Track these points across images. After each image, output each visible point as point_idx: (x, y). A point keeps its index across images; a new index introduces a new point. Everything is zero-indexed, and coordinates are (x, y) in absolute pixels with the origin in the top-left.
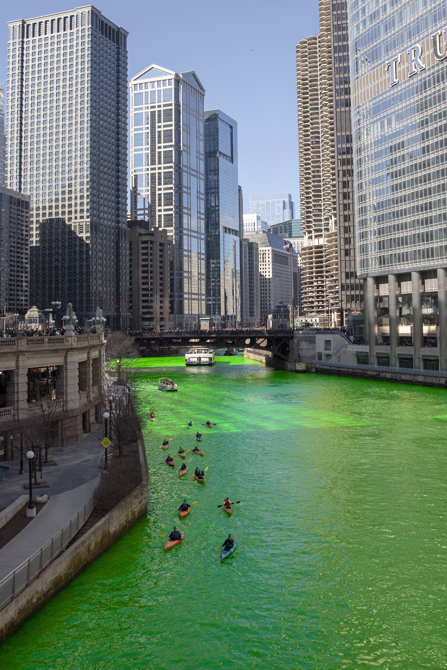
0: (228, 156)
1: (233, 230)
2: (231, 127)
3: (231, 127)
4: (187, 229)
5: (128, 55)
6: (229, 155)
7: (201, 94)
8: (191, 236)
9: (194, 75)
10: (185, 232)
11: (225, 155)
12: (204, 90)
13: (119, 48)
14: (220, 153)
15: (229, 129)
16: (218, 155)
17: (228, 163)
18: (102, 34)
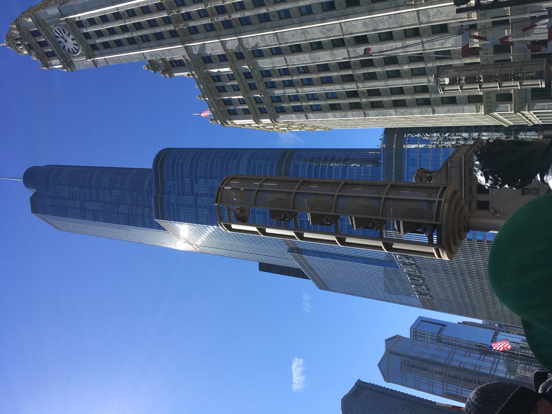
0: (442, 328)
1: (494, 335)
2: (422, 321)
3: (422, 321)
4: (491, 370)
5: (372, 383)
6: (440, 327)
7: (399, 338)
8: (496, 369)
9: (387, 341)
10: (492, 373)
11: (440, 330)
12: (398, 335)
13: (368, 389)
14: (439, 333)
15: (424, 323)
16: (440, 335)
17: (446, 328)
18: (358, 397)
